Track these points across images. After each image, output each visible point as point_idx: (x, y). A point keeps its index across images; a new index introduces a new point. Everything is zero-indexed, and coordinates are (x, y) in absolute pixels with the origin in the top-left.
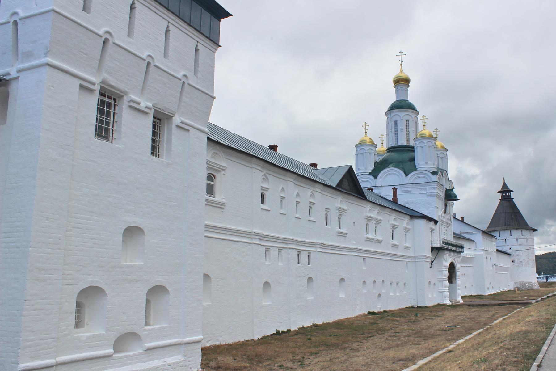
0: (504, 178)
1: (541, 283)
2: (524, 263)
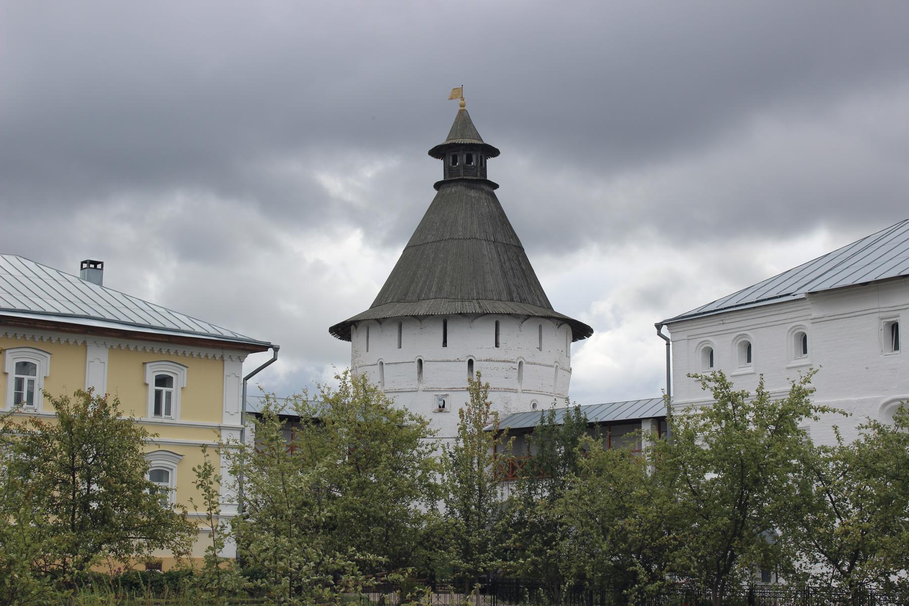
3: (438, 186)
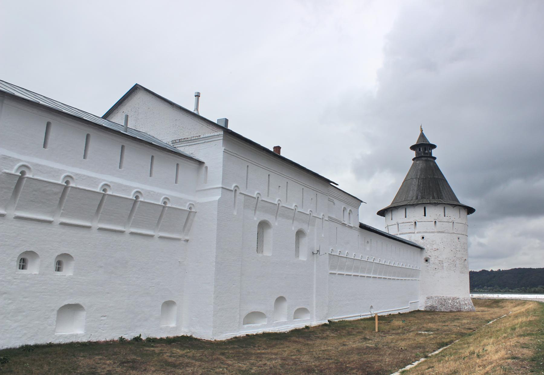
0: (421, 126)
1: (483, 299)
2: (445, 265)
3: (413, 160)
